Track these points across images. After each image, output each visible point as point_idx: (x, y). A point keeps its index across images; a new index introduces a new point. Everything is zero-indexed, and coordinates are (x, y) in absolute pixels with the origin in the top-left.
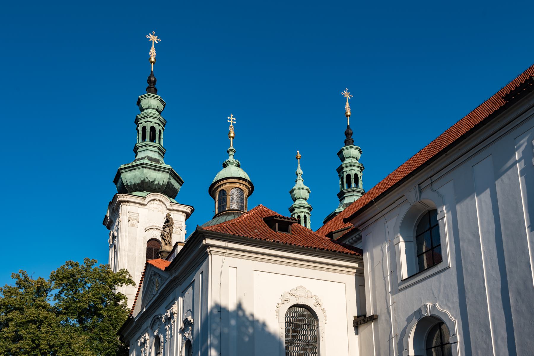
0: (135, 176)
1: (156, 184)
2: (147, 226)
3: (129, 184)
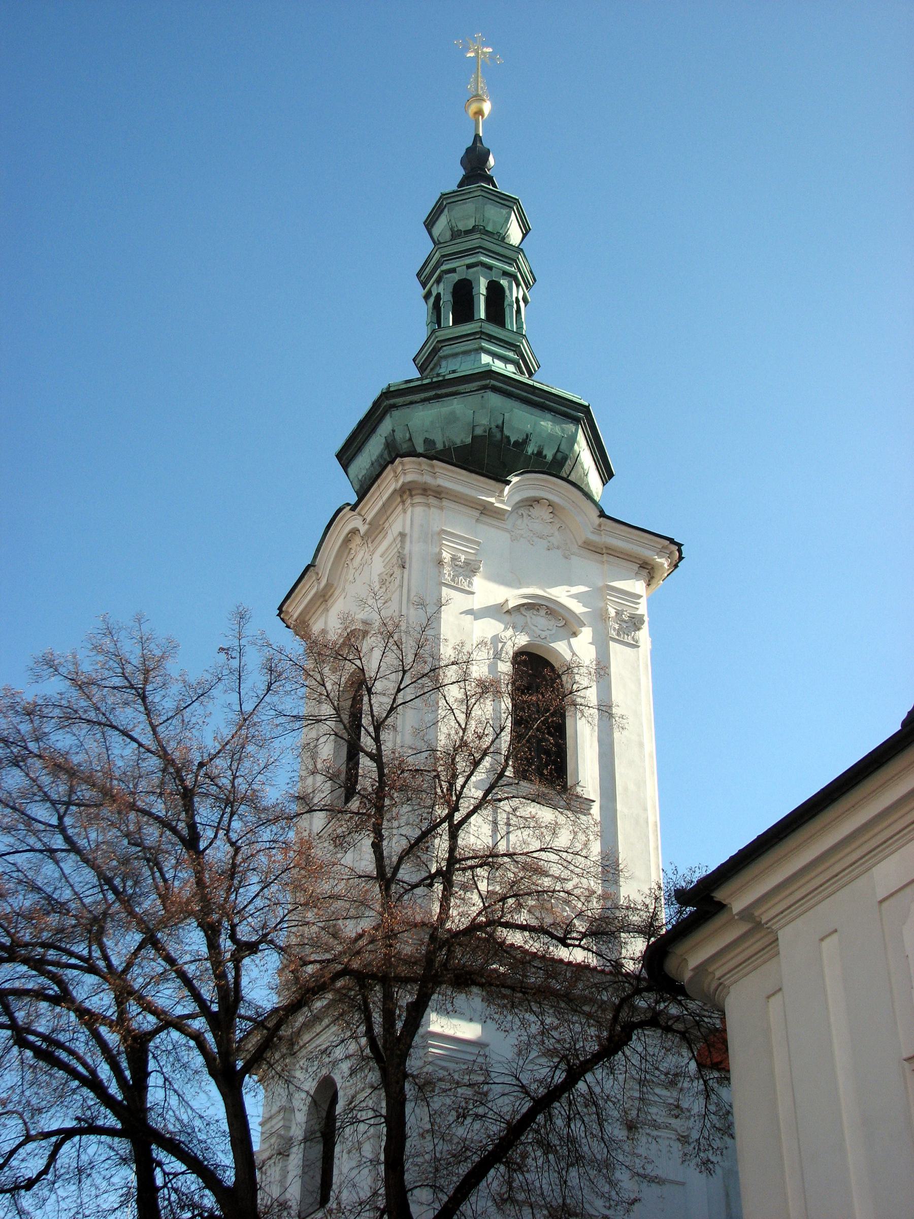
1: (530, 457)
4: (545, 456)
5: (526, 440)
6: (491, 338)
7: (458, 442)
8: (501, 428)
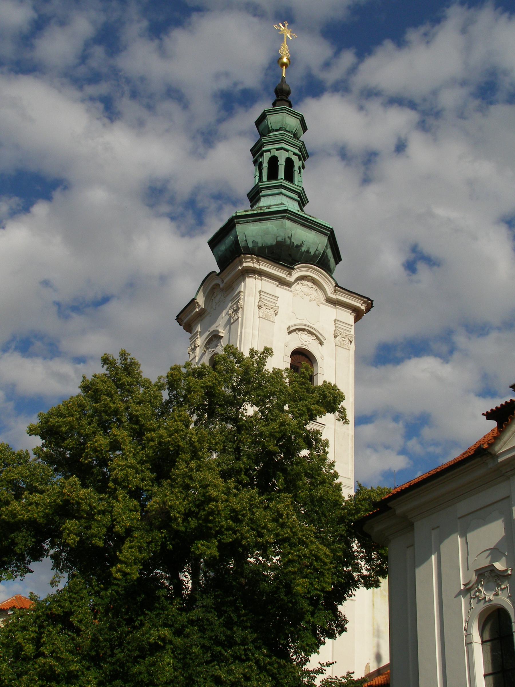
0: (266, 233)
1: (303, 252)
2: (293, 322)
3: (250, 245)
4: (311, 252)
5: (301, 245)
6: (286, 188)
7: (269, 244)
8: (290, 238)
